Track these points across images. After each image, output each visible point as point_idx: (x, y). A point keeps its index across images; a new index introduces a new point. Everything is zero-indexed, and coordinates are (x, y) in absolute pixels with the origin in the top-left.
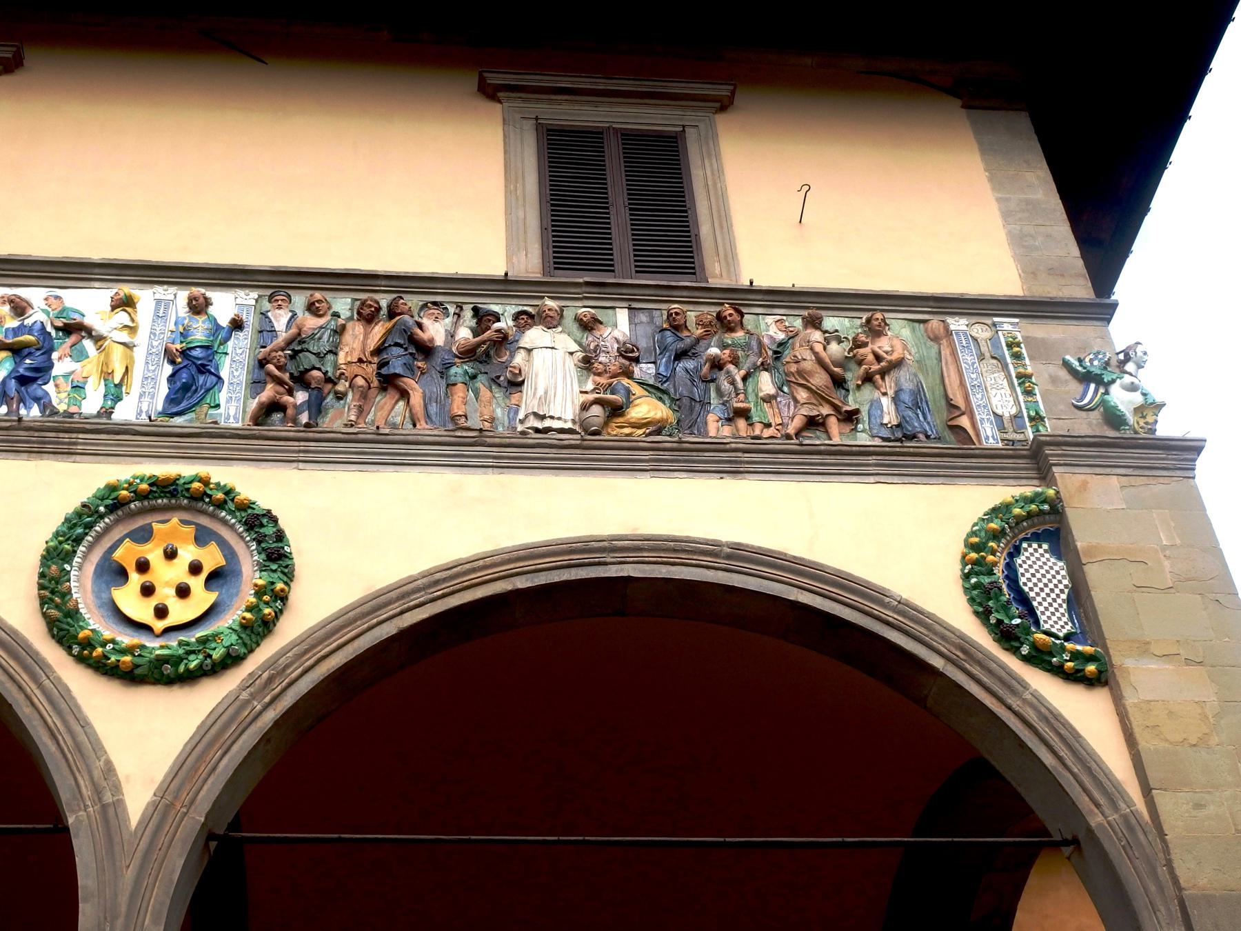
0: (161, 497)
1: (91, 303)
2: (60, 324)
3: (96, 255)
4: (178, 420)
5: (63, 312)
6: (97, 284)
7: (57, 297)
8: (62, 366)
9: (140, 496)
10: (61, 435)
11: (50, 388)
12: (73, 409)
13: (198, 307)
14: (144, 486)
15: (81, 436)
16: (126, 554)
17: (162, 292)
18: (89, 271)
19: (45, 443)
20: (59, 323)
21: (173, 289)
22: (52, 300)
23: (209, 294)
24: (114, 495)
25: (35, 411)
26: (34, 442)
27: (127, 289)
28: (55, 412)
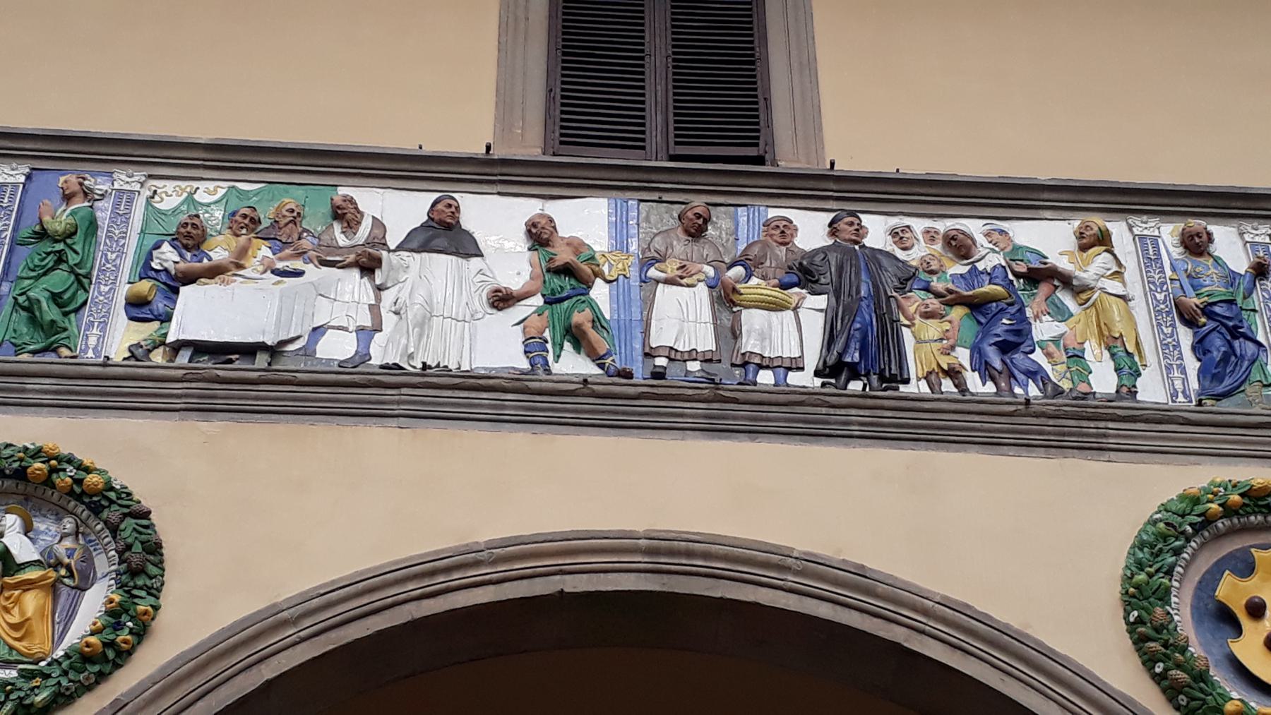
0: (1255, 513)
1: (1050, 238)
2: (1024, 270)
3: (1043, 175)
4: (1225, 405)
5: (1016, 252)
6: (1048, 214)
7: (1002, 232)
8: (1044, 329)
9: (1229, 511)
10: (1085, 423)
11: (1038, 356)
12: (1083, 388)
13: (1196, 245)
14: (1235, 498)
15: (1111, 425)
16: (1231, 590)
17: (1147, 226)
18: (1035, 196)
19: (1064, 434)
20: (1022, 268)
21: (1153, 221)
22: (996, 236)
23: (1211, 228)
24: (1199, 509)
25: (1033, 391)
26: (1049, 433)
27: (1098, 220)
28: (1058, 392)
